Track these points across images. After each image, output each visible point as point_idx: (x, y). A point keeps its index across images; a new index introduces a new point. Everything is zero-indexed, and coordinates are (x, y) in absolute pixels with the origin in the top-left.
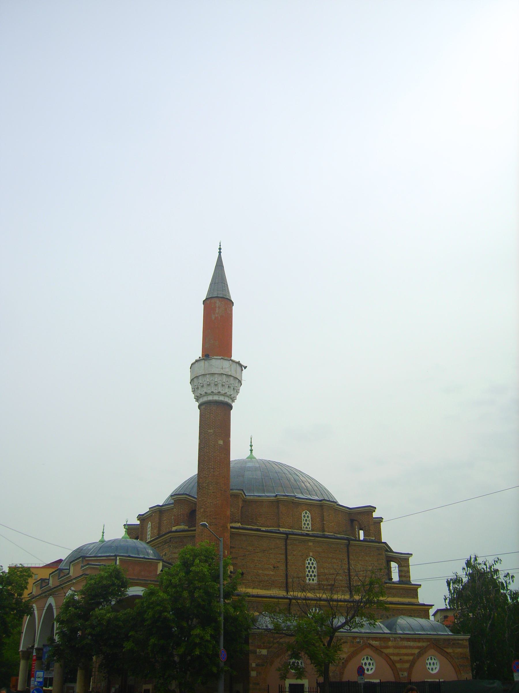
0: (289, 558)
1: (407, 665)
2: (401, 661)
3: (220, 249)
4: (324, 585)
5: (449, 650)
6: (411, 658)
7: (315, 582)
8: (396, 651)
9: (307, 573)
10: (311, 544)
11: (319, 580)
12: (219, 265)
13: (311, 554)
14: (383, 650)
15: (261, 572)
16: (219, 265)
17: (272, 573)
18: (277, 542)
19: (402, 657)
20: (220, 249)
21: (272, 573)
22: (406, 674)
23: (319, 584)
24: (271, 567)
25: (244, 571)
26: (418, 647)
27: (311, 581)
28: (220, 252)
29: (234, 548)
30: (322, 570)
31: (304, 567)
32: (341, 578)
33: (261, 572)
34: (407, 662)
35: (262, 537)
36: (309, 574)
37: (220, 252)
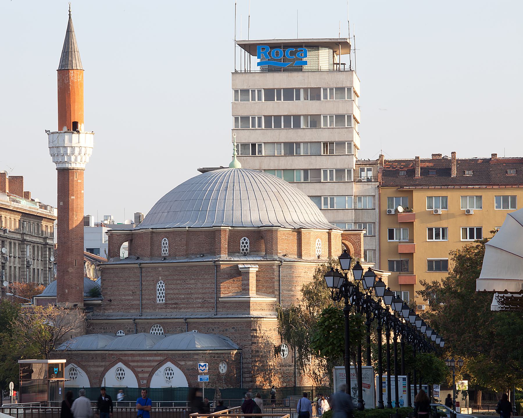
1: (147, 375)
2: (143, 372)
4: (170, 304)
5: (183, 363)
6: (150, 369)
7: (164, 302)
8: (139, 364)
9: (158, 295)
10: (160, 269)
11: (166, 300)
12: (69, 31)
13: (160, 278)
14: (130, 363)
15: (124, 297)
16: (69, 31)
17: (131, 298)
18: (135, 271)
19: (143, 369)
21: (131, 298)
22: (145, 382)
23: (166, 304)
25: (112, 298)
26: (156, 361)
27: (161, 302)
29: (105, 280)
30: (168, 292)
31: (155, 290)
32: (183, 297)
33: (124, 297)
34: (147, 372)
35: (124, 268)
36: (160, 296)
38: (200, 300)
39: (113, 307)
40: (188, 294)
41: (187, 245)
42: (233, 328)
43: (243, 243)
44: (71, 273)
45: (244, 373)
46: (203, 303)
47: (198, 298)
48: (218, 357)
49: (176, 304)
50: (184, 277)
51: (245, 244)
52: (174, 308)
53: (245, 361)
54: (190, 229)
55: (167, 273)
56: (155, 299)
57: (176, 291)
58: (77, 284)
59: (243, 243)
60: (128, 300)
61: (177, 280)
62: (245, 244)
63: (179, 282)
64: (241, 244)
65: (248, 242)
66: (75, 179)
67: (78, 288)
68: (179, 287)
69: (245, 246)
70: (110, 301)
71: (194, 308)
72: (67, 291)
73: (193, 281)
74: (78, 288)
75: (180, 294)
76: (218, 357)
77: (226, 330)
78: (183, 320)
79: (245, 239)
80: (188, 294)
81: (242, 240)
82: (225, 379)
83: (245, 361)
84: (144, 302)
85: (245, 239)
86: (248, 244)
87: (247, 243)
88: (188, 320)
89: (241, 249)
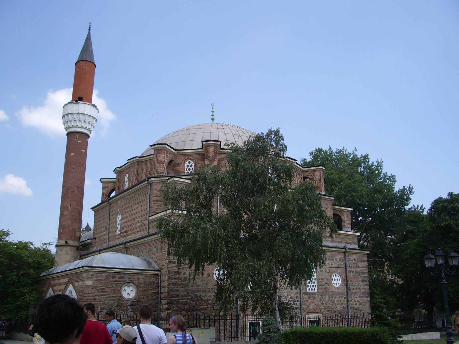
0: (111, 218)
3: (90, 28)
12: (88, 39)
16: (88, 39)
17: (104, 233)
20: (90, 28)
23: (121, 233)
24: (104, 228)
28: (89, 30)
33: (101, 234)
37: (89, 30)
38: (139, 224)
39: (96, 244)
40: (133, 220)
41: (138, 174)
42: (155, 247)
43: (188, 166)
44: (66, 215)
45: (161, 299)
46: (141, 226)
47: (137, 222)
48: (120, 278)
49: (126, 232)
50: (130, 205)
51: (189, 167)
52: (125, 236)
53: (162, 284)
54: (141, 159)
55: (122, 204)
56: (115, 231)
57: (126, 220)
58: (70, 225)
59: (188, 166)
60: (103, 235)
61: (127, 208)
62: (189, 167)
63: (128, 210)
64: (186, 167)
65: (193, 165)
66: (76, 140)
67: (71, 228)
68: (128, 214)
69: (189, 169)
70: (95, 238)
71: (135, 233)
72: (61, 230)
73: (136, 206)
74: (71, 228)
75: (128, 221)
76: (120, 278)
77: (151, 250)
78: (122, 246)
79: (189, 163)
80: (133, 220)
81: (187, 163)
82: (131, 305)
83: (162, 284)
84: (110, 235)
85: (189, 163)
86: (193, 167)
87: (191, 166)
88: (127, 245)
89: (186, 172)
